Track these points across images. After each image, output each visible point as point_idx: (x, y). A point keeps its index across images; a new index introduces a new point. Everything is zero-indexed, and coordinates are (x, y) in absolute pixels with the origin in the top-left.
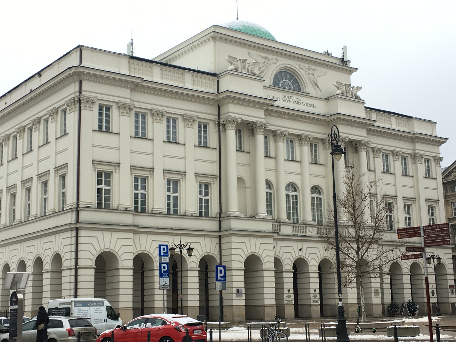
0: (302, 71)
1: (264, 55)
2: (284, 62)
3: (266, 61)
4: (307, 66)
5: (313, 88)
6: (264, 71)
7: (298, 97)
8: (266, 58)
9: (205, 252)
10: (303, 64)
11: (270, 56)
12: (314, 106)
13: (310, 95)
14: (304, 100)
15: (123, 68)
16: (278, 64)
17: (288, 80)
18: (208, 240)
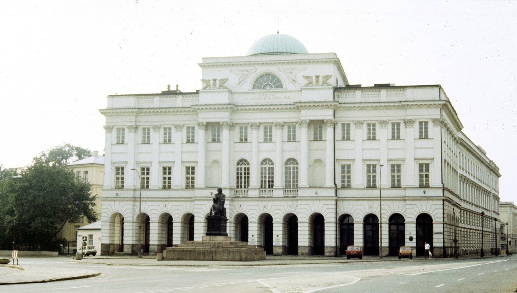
0: (281, 73)
1: (243, 68)
2: (262, 70)
3: (245, 72)
4: (286, 67)
5: (291, 83)
6: (243, 80)
7: (273, 94)
8: (245, 70)
9: (185, 210)
10: (281, 67)
11: (249, 68)
12: (289, 98)
13: (289, 89)
14: (278, 95)
15: (131, 103)
16: (257, 72)
17: (269, 81)
18: (188, 203)
